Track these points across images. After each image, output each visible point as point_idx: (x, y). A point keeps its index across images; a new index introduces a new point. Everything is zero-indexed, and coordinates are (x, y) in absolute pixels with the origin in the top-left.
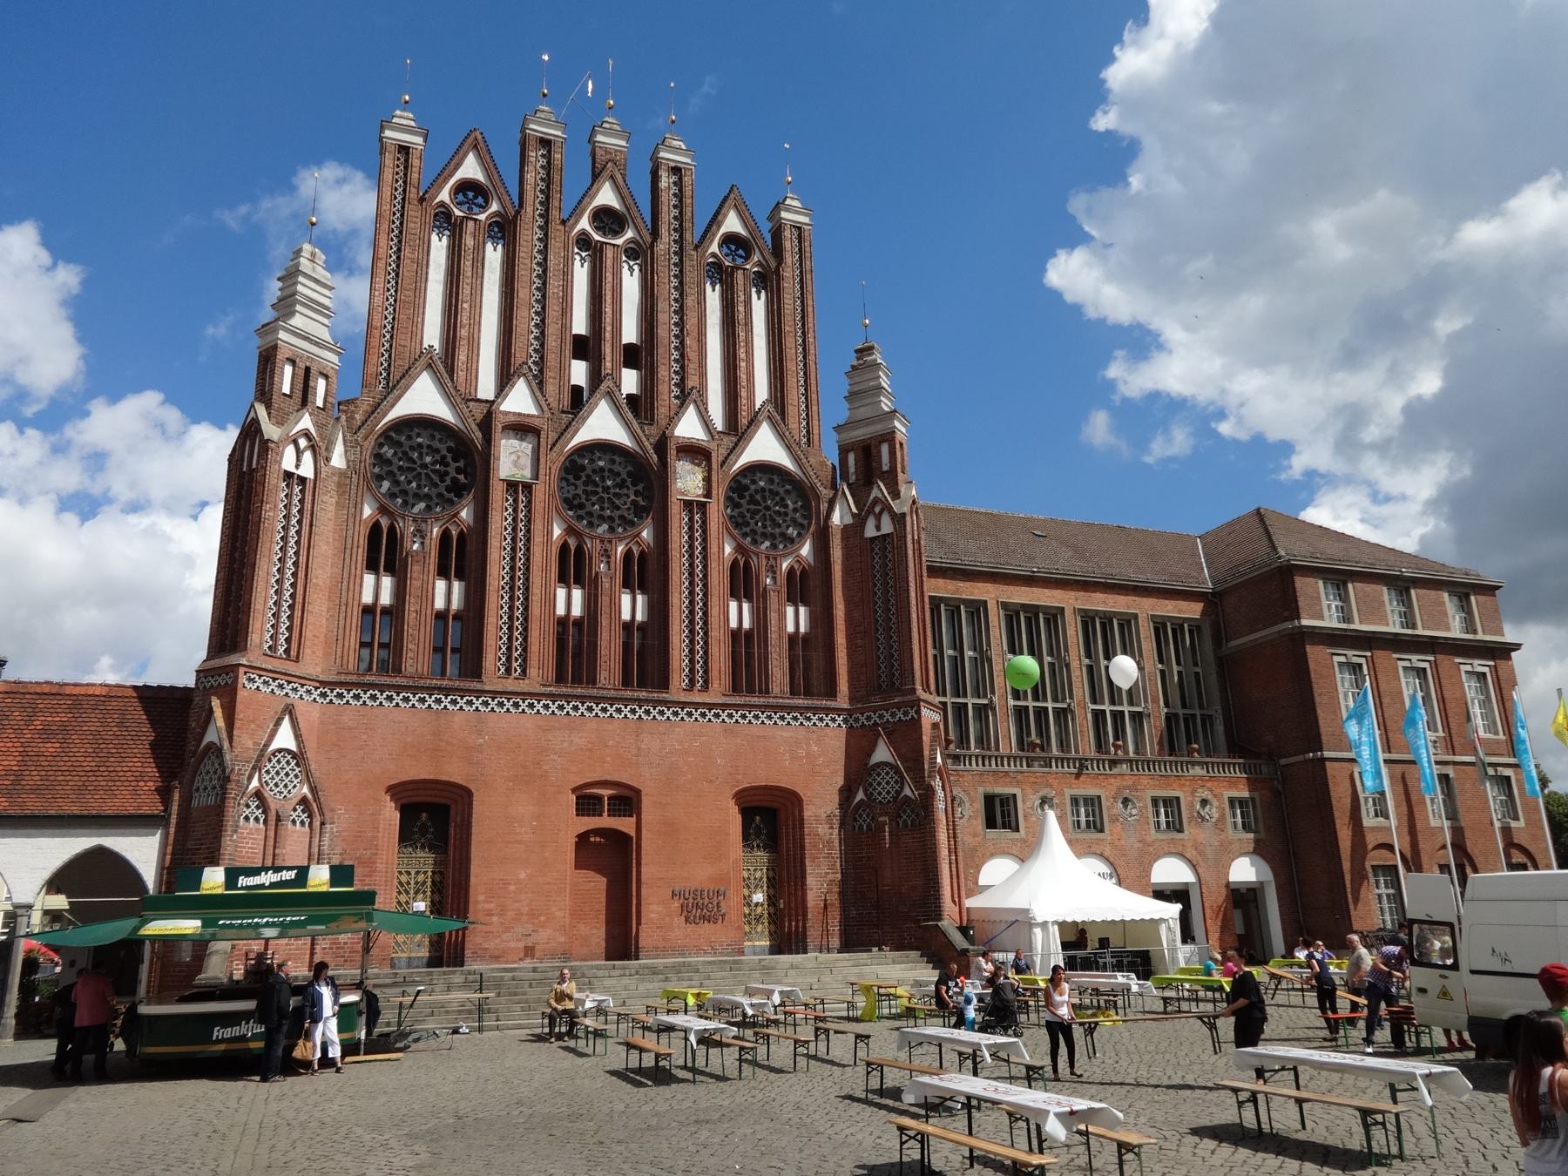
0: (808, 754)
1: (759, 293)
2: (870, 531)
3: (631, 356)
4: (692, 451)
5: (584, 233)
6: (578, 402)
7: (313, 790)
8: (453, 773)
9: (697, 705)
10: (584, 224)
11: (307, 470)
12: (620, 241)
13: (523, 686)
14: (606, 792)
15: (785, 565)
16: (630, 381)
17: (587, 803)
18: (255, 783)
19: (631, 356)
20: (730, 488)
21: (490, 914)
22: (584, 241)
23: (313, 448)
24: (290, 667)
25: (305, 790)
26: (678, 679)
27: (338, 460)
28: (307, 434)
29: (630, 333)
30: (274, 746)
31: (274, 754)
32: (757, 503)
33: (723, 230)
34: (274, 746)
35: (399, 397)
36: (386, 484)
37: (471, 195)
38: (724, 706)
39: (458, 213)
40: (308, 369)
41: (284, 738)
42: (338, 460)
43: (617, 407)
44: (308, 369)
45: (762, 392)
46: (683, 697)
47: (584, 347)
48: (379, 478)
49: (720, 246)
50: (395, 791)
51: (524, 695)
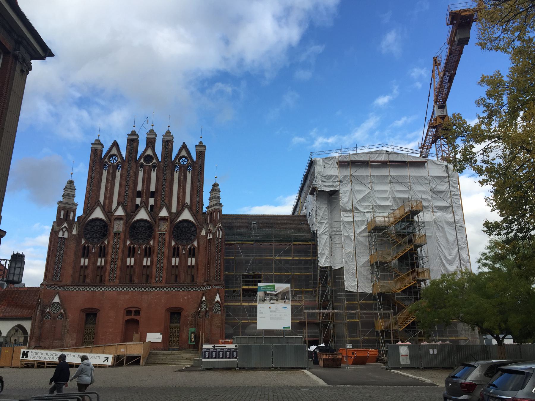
0: (188, 298)
1: (189, 171)
2: (209, 238)
3: (152, 195)
4: (164, 219)
5: (142, 163)
6: (137, 208)
7: (64, 311)
8: (96, 306)
9: (158, 287)
10: (142, 161)
11: (66, 236)
12: (151, 164)
13: (114, 284)
14: (133, 309)
15: (188, 247)
16: (152, 201)
17: (129, 312)
18: (48, 310)
19: (152, 195)
20: (174, 228)
21: (102, 340)
22: (142, 166)
23: (67, 230)
24: (59, 283)
25: (62, 311)
26: (153, 280)
27: (74, 232)
28: (65, 227)
29: (153, 188)
30: (54, 301)
31: (53, 303)
32: (182, 231)
33: (180, 155)
34: (54, 301)
35: (91, 215)
36: (88, 236)
37: (111, 159)
38: (165, 287)
39: (109, 164)
40: (68, 211)
41: (57, 299)
42: (74, 232)
43: (146, 209)
44: (68, 211)
45: (188, 200)
46: (154, 285)
47: (139, 194)
48: (86, 234)
49: (179, 161)
50: (83, 310)
51: (114, 286)
